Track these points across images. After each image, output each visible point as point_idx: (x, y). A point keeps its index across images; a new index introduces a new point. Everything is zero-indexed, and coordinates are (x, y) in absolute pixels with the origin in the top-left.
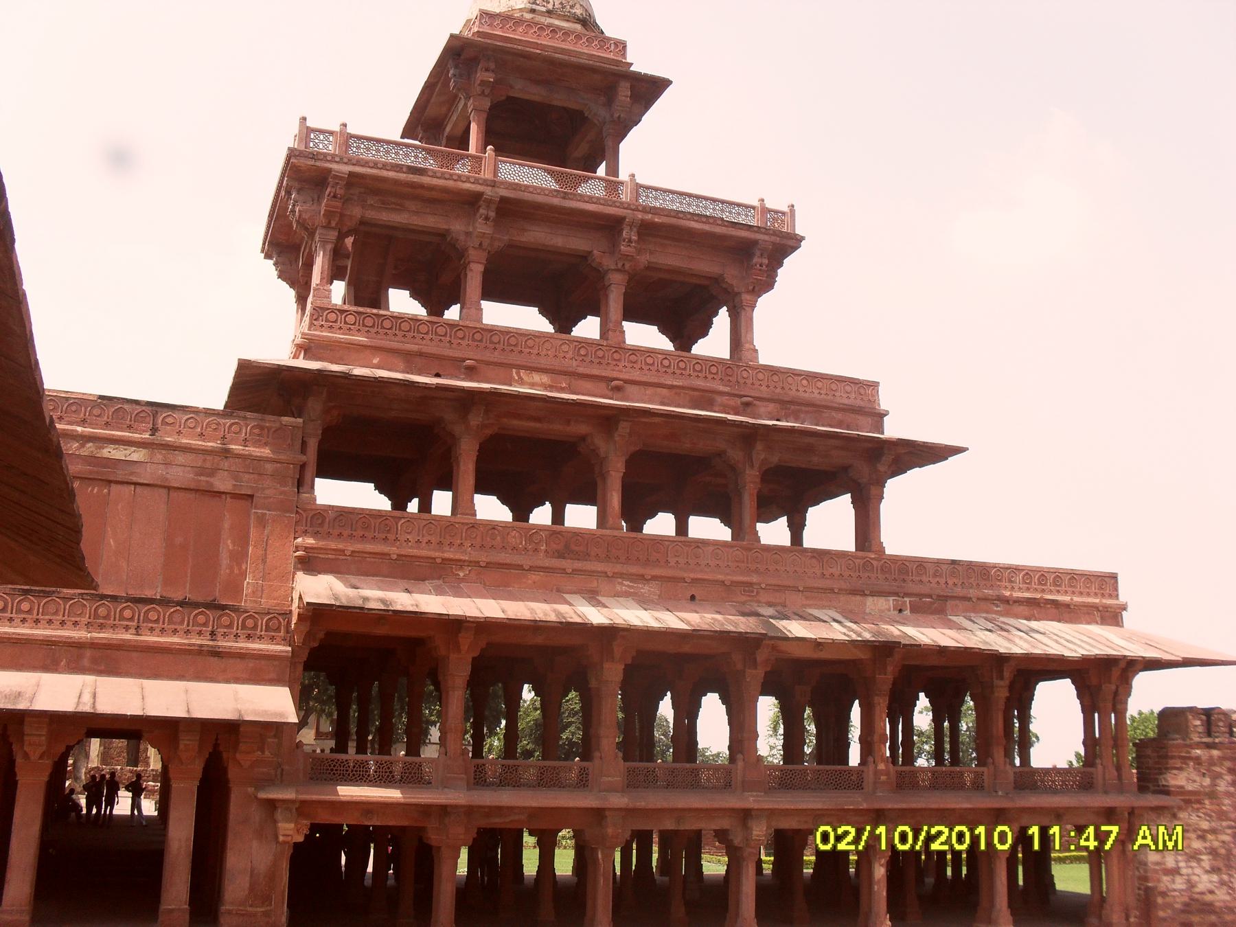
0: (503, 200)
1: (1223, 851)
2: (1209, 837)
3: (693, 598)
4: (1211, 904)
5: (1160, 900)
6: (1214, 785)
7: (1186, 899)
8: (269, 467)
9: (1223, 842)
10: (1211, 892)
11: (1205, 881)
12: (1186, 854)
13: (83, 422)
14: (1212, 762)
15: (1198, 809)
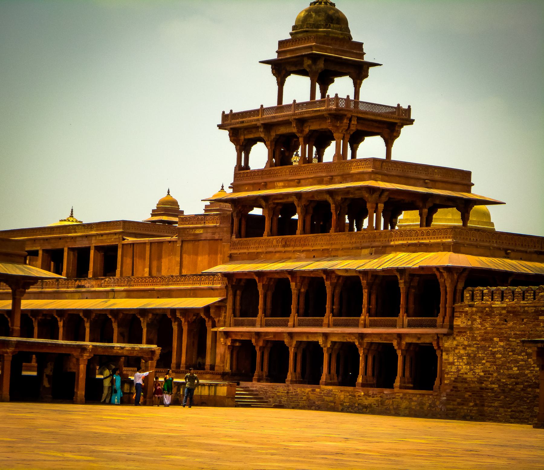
0: (262, 124)
1: (472, 355)
2: (468, 348)
3: (314, 257)
4: (465, 379)
5: (446, 376)
6: (472, 324)
7: (456, 376)
8: (225, 229)
9: (473, 351)
10: (466, 373)
11: (464, 368)
12: (458, 356)
13: (192, 224)
14: (472, 314)
15: (464, 336)
